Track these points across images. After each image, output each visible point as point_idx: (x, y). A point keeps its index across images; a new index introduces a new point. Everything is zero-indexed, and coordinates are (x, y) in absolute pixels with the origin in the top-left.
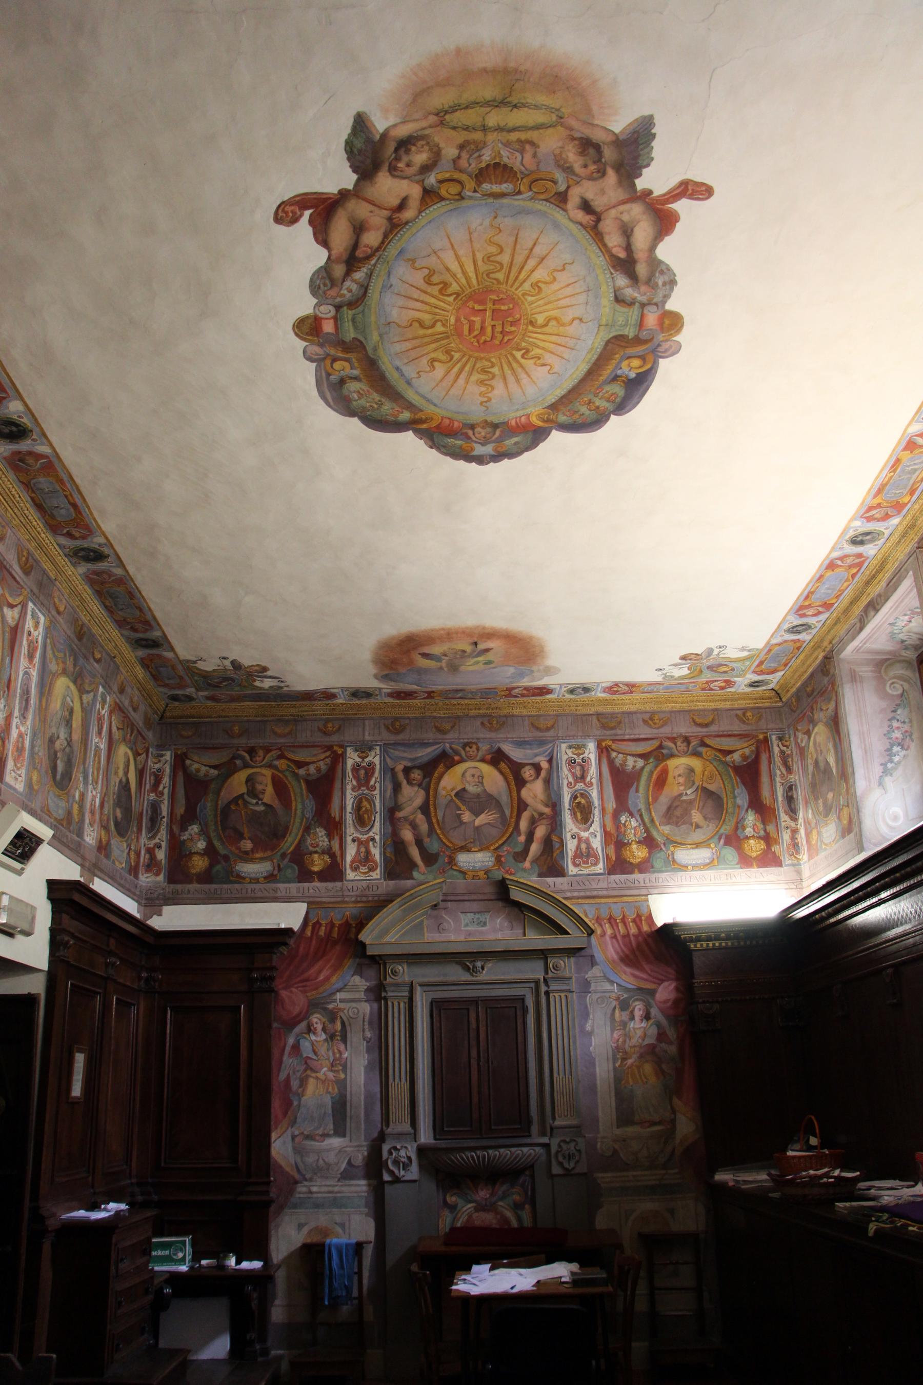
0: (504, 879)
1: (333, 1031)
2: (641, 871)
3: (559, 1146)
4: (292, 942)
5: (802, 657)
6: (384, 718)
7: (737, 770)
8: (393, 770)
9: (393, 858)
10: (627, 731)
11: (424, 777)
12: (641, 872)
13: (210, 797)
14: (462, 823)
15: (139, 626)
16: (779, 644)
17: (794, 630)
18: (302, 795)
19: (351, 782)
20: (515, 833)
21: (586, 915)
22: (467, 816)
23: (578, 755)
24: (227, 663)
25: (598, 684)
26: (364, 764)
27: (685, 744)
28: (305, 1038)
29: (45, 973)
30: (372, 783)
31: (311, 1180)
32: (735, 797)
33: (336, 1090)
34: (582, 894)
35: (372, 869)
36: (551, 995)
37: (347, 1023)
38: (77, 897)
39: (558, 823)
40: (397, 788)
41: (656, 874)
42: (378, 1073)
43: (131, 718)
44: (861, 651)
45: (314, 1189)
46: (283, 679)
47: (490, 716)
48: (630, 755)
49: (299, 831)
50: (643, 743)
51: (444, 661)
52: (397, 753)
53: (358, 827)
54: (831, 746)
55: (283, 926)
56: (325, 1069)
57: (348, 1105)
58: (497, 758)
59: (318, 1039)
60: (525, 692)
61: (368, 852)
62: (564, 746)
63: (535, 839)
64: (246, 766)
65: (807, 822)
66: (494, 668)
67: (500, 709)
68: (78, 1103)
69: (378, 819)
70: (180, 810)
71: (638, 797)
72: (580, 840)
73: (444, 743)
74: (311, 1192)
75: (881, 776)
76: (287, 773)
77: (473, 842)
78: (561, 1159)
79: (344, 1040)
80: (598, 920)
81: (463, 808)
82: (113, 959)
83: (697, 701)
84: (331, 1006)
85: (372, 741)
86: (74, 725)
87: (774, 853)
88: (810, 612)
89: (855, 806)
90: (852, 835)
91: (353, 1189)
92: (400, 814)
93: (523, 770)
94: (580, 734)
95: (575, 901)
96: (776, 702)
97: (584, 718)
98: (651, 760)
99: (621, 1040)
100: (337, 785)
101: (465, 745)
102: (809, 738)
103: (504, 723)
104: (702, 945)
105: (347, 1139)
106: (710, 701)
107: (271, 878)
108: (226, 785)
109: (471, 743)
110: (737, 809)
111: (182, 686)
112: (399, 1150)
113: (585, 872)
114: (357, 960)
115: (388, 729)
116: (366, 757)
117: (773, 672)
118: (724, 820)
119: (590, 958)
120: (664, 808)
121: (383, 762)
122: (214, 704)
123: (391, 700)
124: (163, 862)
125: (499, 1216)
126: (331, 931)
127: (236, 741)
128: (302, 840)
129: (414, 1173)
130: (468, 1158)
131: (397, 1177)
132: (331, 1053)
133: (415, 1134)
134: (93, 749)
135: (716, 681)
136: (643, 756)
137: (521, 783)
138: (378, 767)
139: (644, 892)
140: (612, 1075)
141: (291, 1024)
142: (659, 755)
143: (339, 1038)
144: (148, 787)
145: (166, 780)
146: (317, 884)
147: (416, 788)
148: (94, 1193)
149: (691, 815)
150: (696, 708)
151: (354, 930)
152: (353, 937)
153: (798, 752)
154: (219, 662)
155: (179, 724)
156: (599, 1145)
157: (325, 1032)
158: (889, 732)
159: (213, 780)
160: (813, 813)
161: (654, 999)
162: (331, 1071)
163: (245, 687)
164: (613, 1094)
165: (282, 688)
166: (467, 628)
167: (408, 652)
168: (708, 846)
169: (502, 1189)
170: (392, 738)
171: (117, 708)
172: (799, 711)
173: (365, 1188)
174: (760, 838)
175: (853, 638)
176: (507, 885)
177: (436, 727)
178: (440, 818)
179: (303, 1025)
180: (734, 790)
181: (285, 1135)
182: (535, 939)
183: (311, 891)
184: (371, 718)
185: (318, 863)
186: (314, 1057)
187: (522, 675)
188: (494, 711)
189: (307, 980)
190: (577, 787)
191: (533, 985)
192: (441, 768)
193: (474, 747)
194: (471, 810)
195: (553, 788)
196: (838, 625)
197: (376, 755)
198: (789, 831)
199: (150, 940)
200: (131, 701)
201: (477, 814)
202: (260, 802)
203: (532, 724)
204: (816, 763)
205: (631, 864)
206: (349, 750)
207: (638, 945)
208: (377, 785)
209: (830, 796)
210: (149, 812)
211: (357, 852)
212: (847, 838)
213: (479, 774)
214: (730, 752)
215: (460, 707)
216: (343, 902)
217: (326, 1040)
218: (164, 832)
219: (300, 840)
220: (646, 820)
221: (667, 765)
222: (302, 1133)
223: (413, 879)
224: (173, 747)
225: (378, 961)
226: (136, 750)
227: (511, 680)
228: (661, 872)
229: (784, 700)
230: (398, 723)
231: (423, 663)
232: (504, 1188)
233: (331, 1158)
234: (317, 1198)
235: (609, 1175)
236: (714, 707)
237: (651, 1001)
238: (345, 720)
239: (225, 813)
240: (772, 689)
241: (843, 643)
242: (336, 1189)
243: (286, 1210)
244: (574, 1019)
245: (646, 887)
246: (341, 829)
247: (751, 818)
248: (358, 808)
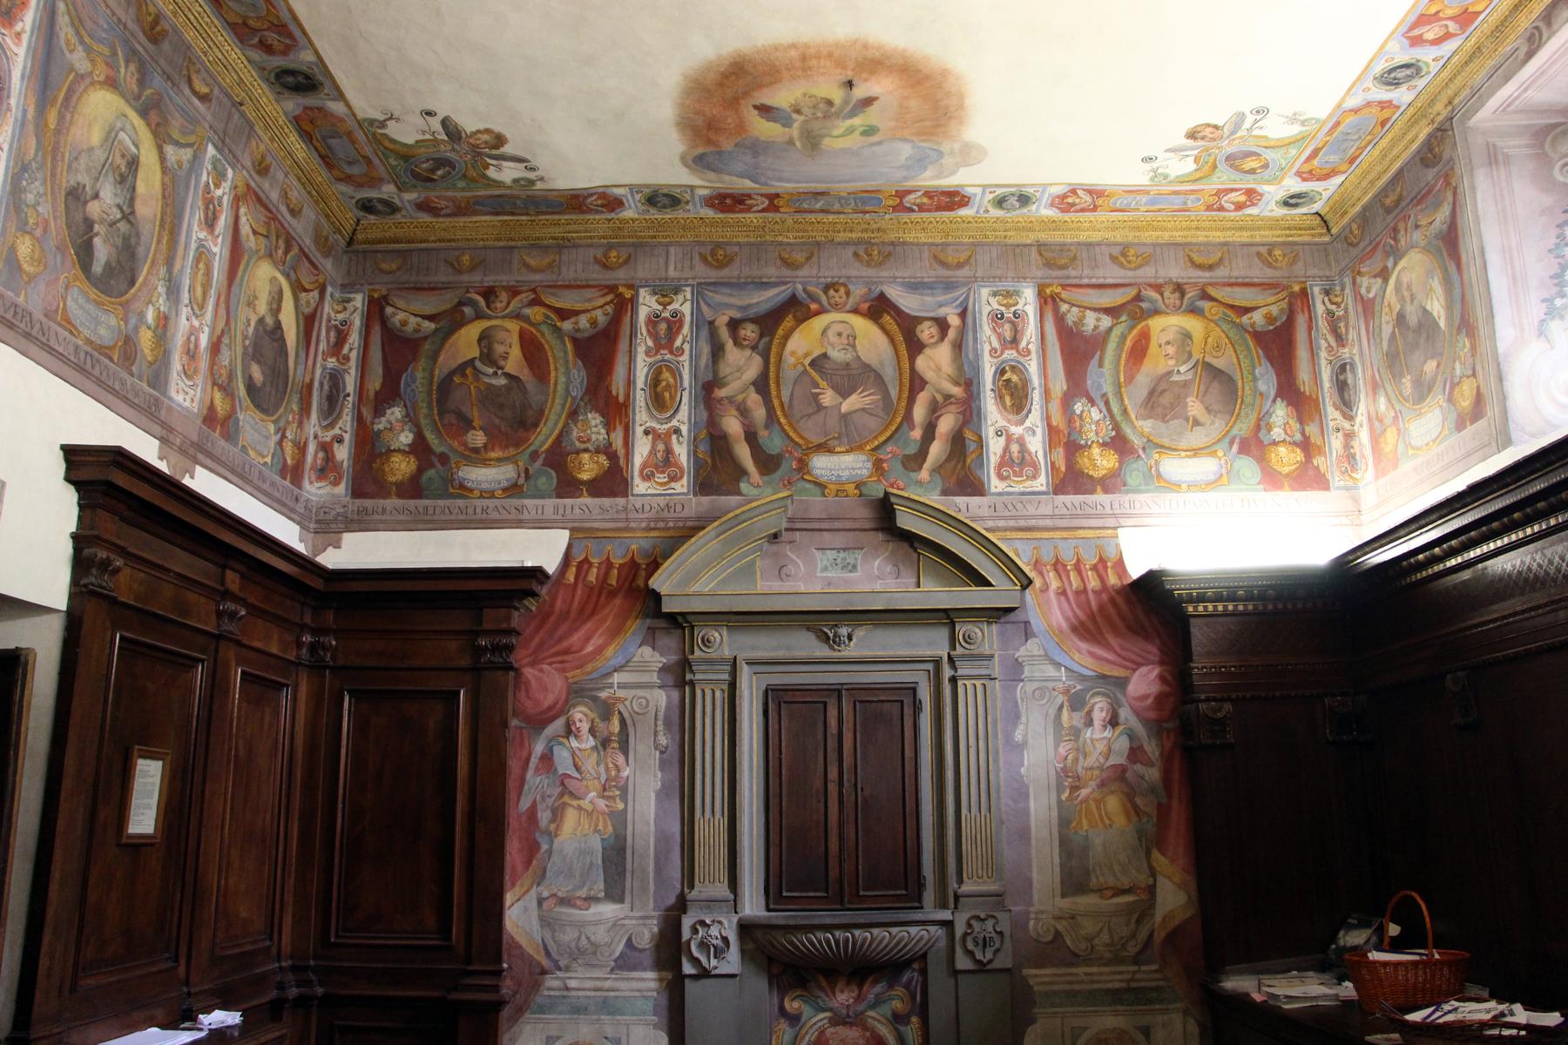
0: (887, 494)
1: (606, 734)
2: (1106, 490)
3: (969, 925)
4: (544, 591)
5: (1384, 143)
6: (702, 244)
7: (1259, 337)
8: (711, 323)
9: (709, 461)
10: (1086, 272)
11: (761, 336)
12: (1106, 491)
13: (422, 363)
14: (820, 407)
15: (272, 38)
16: (1355, 111)
17: (1391, 78)
18: (567, 362)
19: (644, 342)
20: (905, 425)
21: (1018, 555)
22: (828, 397)
23: (1008, 306)
24: (435, 124)
25: (1045, 186)
26: (666, 314)
27: (1177, 295)
28: (561, 744)
29: (63, 614)
30: (678, 343)
31: (567, 969)
32: (1255, 380)
33: (610, 829)
34: (1012, 523)
35: (673, 479)
36: (960, 683)
37: (629, 722)
38: (121, 479)
39: (975, 411)
40: (717, 351)
41: (1130, 496)
42: (677, 801)
43: (286, 225)
44: (1513, 107)
45: (573, 984)
46: (534, 163)
47: (869, 243)
48: (1090, 309)
49: (560, 417)
50: (1110, 292)
51: (796, 125)
52: (719, 298)
53: (652, 409)
54: (1436, 284)
55: (529, 564)
56: (593, 794)
57: (629, 852)
58: (878, 308)
59: (583, 746)
60: (925, 200)
61: (669, 451)
62: (985, 292)
63: (937, 435)
64: (479, 316)
65: (1375, 419)
66: (880, 143)
67: (884, 231)
68: (152, 845)
69: (685, 400)
70: (375, 383)
71: (1101, 375)
72: (1009, 439)
73: (794, 283)
74: (567, 989)
75: (1543, 320)
76: (544, 328)
77: (839, 438)
78: (970, 946)
79: (624, 748)
80: (1037, 565)
81: (823, 384)
82: (230, 606)
83: (1197, 228)
84: (603, 695)
85: (679, 279)
86: (141, 188)
87: (1317, 468)
88: (1431, 33)
89: (1493, 372)
90: (1481, 423)
91: (635, 985)
92: (721, 393)
93: (919, 328)
94: (1011, 274)
95: (1000, 534)
96: (1321, 235)
97: (1018, 251)
98: (1124, 318)
99: (1070, 757)
100: (623, 346)
101: (826, 288)
102: (1386, 280)
103: (890, 254)
104: (1205, 607)
105: (627, 905)
106: (1217, 229)
107: (513, 490)
108: (447, 345)
109: (837, 283)
110: (1258, 401)
111: (374, 182)
112: (709, 926)
113: (1018, 488)
114: (648, 621)
115: (704, 260)
116: (669, 304)
117: (1326, 177)
118: (1238, 415)
119: (1022, 625)
120: (1144, 393)
121: (697, 312)
122: (430, 220)
123: (709, 213)
124: (345, 464)
125: (868, 1034)
126: (607, 574)
127: (466, 278)
128: (564, 432)
129: (732, 962)
130: (820, 942)
131: (704, 968)
132: (602, 769)
133: (735, 901)
134: (193, 246)
135: (1232, 190)
136: (1108, 311)
137: (916, 347)
138: (688, 319)
139: (1110, 522)
140: (1055, 814)
141: (540, 721)
142: (1136, 309)
143: (616, 745)
144: (323, 346)
145: (354, 338)
146: (587, 500)
147: (748, 352)
148: (189, 994)
149: (1186, 405)
150: (1194, 241)
151: (643, 573)
152: (641, 583)
153: (1360, 309)
154: (420, 121)
155: (376, 252)
156: (1032, 923)
157: (594, 736)
158: (1557, 246)
159: (425, 338)
160: (1389, 400)
161: (1124, 694)
162: (603, 797)
163: (473, 180)
164: (1056, 843)
165: (532, 182)
166: (837, 45)
167: (734, 103)
168: (1213, 454)
169: (874, 990)
170: (712, 275)
171: (247, 195)
172: (1362, 245)
173: (653, 985)
174: (1295, 444)
175: (1507, 79)
176: (892, 504)
177: (782, 259)
178: (785, 399)
179: (558, 725)
180: (1254, 367)
181: (527, 897)
182: (938, 593)
183: (577, 511)
184: (678, 244)
185: (588, 468)
186: (576, 775)
187: (921, 162)
188: (876, 235)
189: (566, 652)
190: (1005, 355)
191: (930, 667)
192: (788, 322)
193: (842, 290)
194: (835, 388)
195: (967, 355)
196: (1477, 61)
197: (686, 300)
198: (1340, 434)
199: (318, 583)
200: (285, 195)
201: (844, 394)
202: (500, 372)
203: (935, 257)
204: (1401, 318)
205: (1091, 477)
206: (642, 292)
207: (1102, 608)
208: (687, 347)
209: (1431, 366)
210: (326, 387)
211: (650, 453)
212: (1470, 429)
213: (849, 331)
214: (1247, 310)
215: (820, 227)
216: (627, 529)
217: (595, 748)
218: (349, 418)
219: (562, 432)
220: (1116, 409)
221: (1148, 326)
222: (555, 895)
223: (739, 493)
224: (367, 288)
225: (678, 622)
226: (298, 280)
227: (905, 173)
228: (1139, 492)
229: (1334, 231)
230: (721, 252)
231: (764, 129)
232: (878, 988)
233: (600, 935)
234: (578, 997)
235: (1048, 971)
236: (1222, 240)
237: (1120, 696)
238: (636, 246)
239: (445, 388)
240: (1317, 213)
241: (1479, 96)
242: (607, 984)
243: (527, 1015)
244: (995, 722)
245: (1114, 516)
246: (627, 415)
247: (1281, 413)
248: (655, 381)
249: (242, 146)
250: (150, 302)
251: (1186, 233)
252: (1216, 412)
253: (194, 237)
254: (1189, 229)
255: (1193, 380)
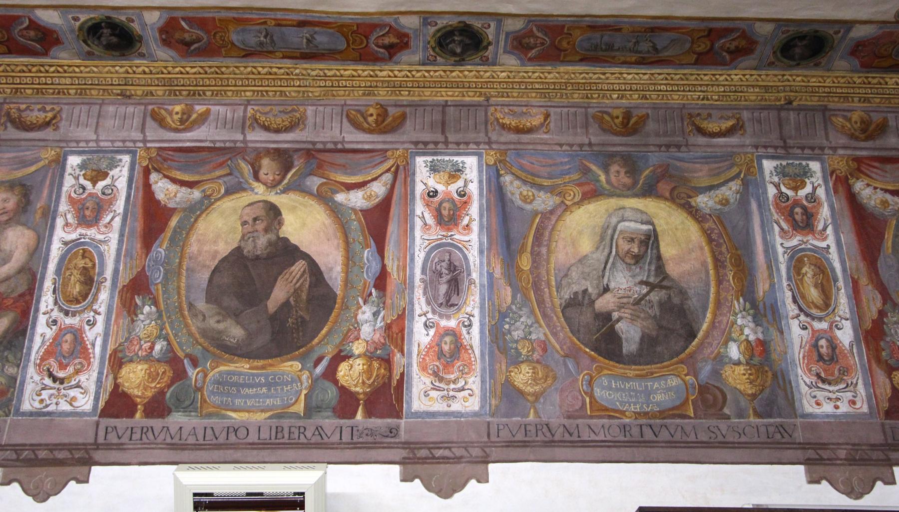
249: (821, 133)
250: (729, 339)
253: (780, 250)
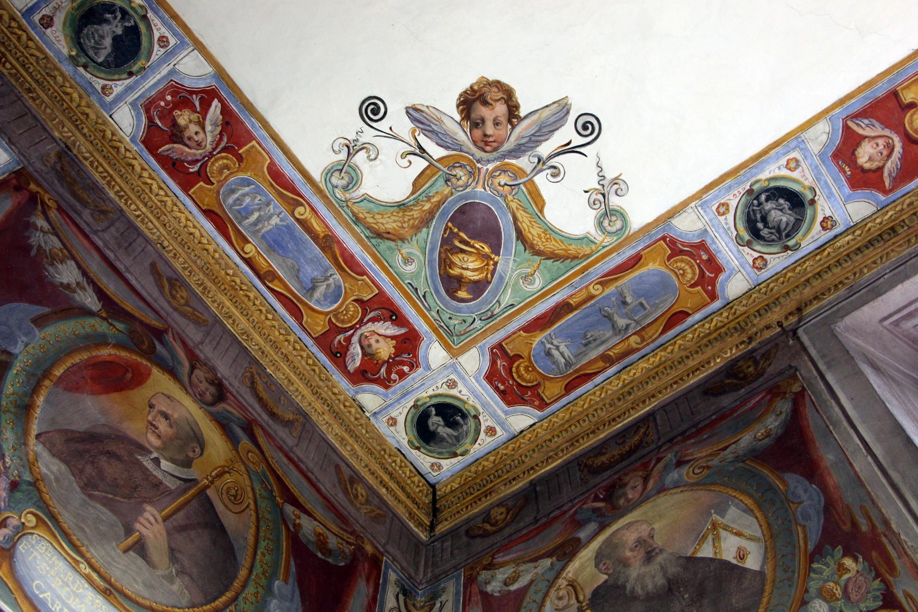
48: (79, 266)
83: (286, 357)
96: (420, 524)
106: (308, 384)
180: (271, 578)
229: (441, 528)
236: (304, 405)
240: (433, 486)
251: (268, 349)
252: (181, 572)
254: (275, 346)
255: (169, 492)
